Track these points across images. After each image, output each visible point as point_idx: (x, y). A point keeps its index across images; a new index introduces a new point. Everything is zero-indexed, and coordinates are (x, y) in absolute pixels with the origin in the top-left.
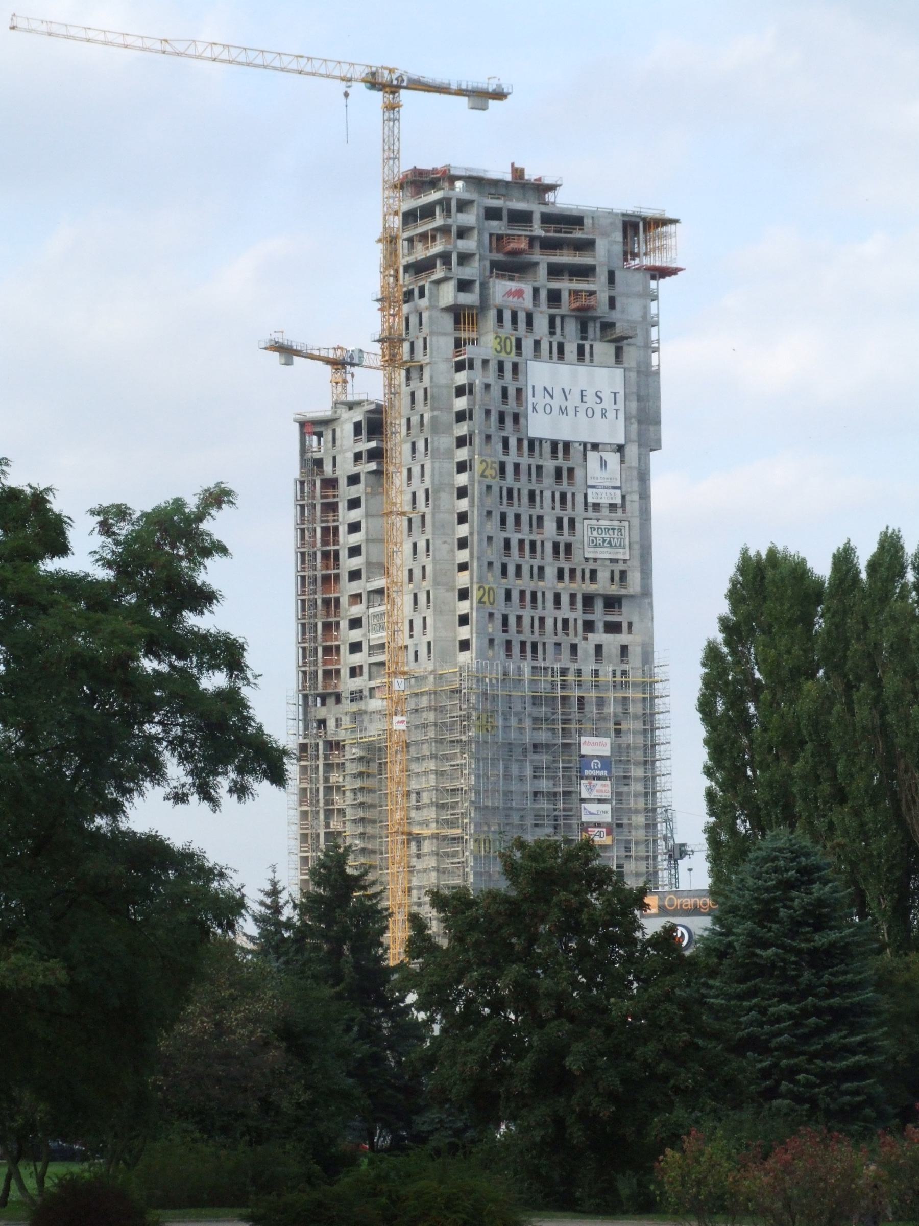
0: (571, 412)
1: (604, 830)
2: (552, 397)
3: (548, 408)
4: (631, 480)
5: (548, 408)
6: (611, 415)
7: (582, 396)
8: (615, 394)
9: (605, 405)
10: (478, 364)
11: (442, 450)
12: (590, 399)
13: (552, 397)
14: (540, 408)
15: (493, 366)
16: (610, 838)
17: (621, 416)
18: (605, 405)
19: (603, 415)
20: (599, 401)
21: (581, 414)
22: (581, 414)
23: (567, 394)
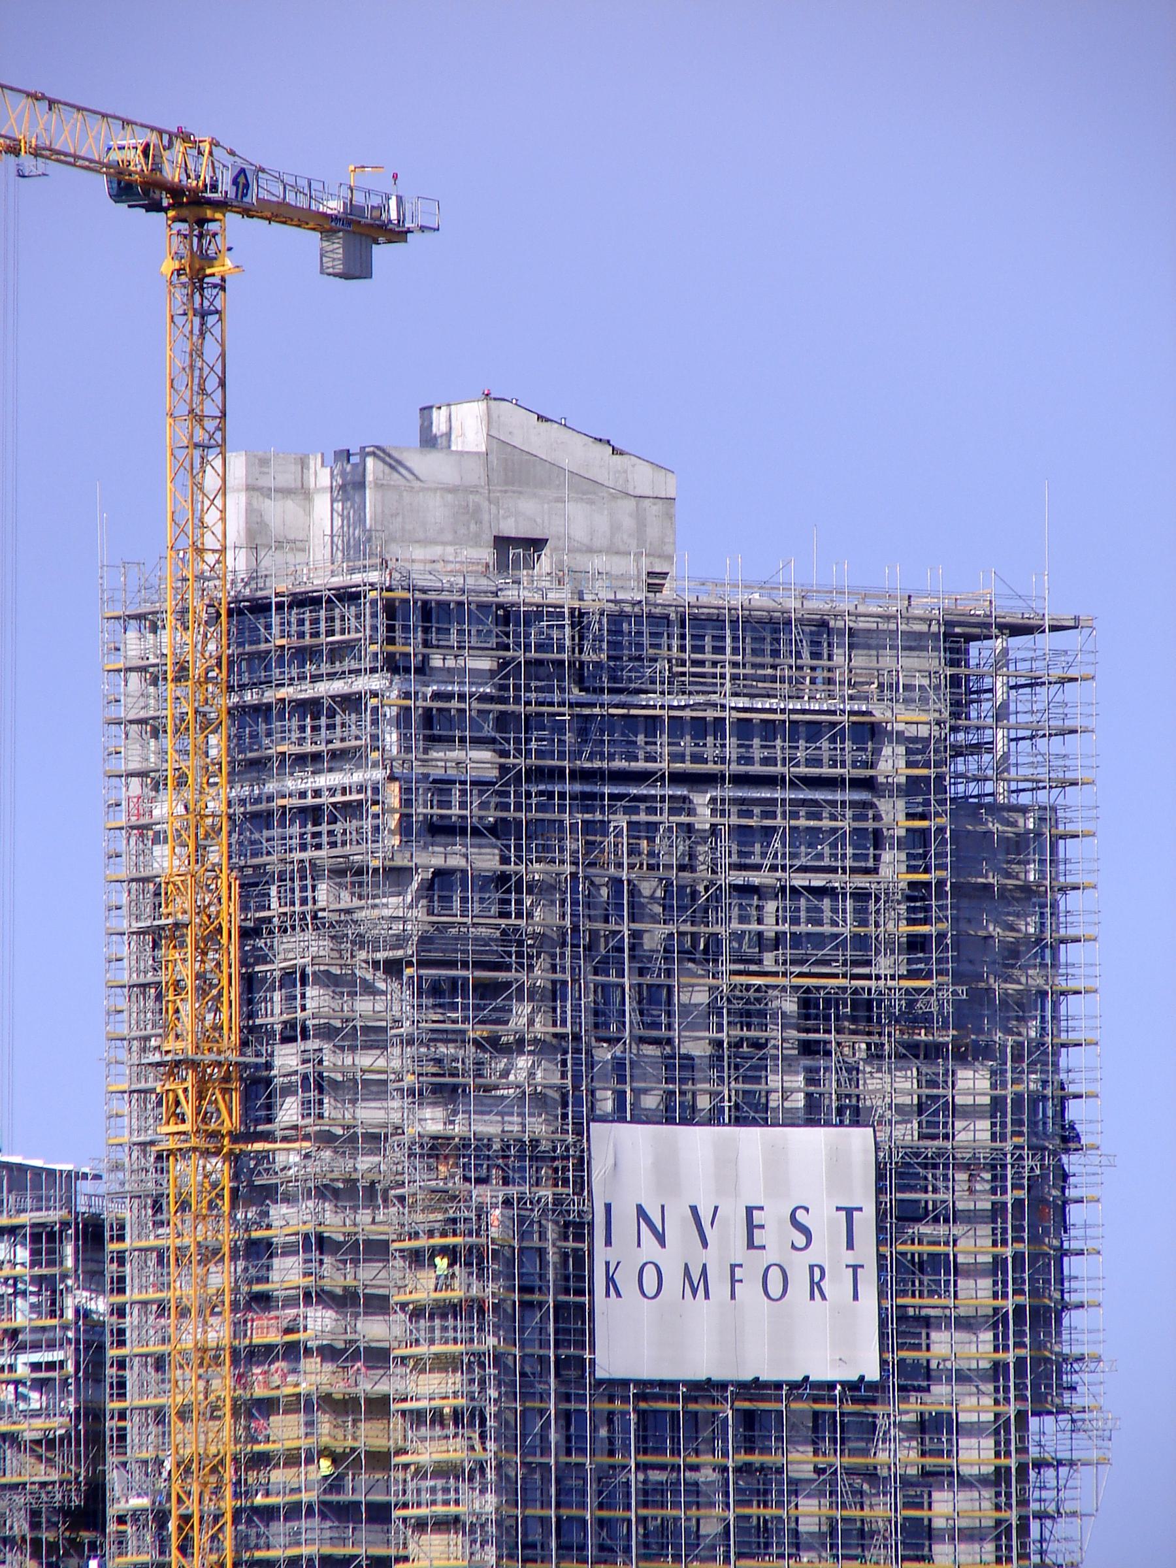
2: (661, 1239)
3: (650, 1275)
5: (650, 1275)
6: (837, 1286)
7: (751, 1227)
8: (849, 1212)
9: (818, 1253)
12: (775, 1235)
13: (661, 1239)
14: (626, 1279)
18: (818, 1253)
19: (816, 1288)
20: (801, 1240)
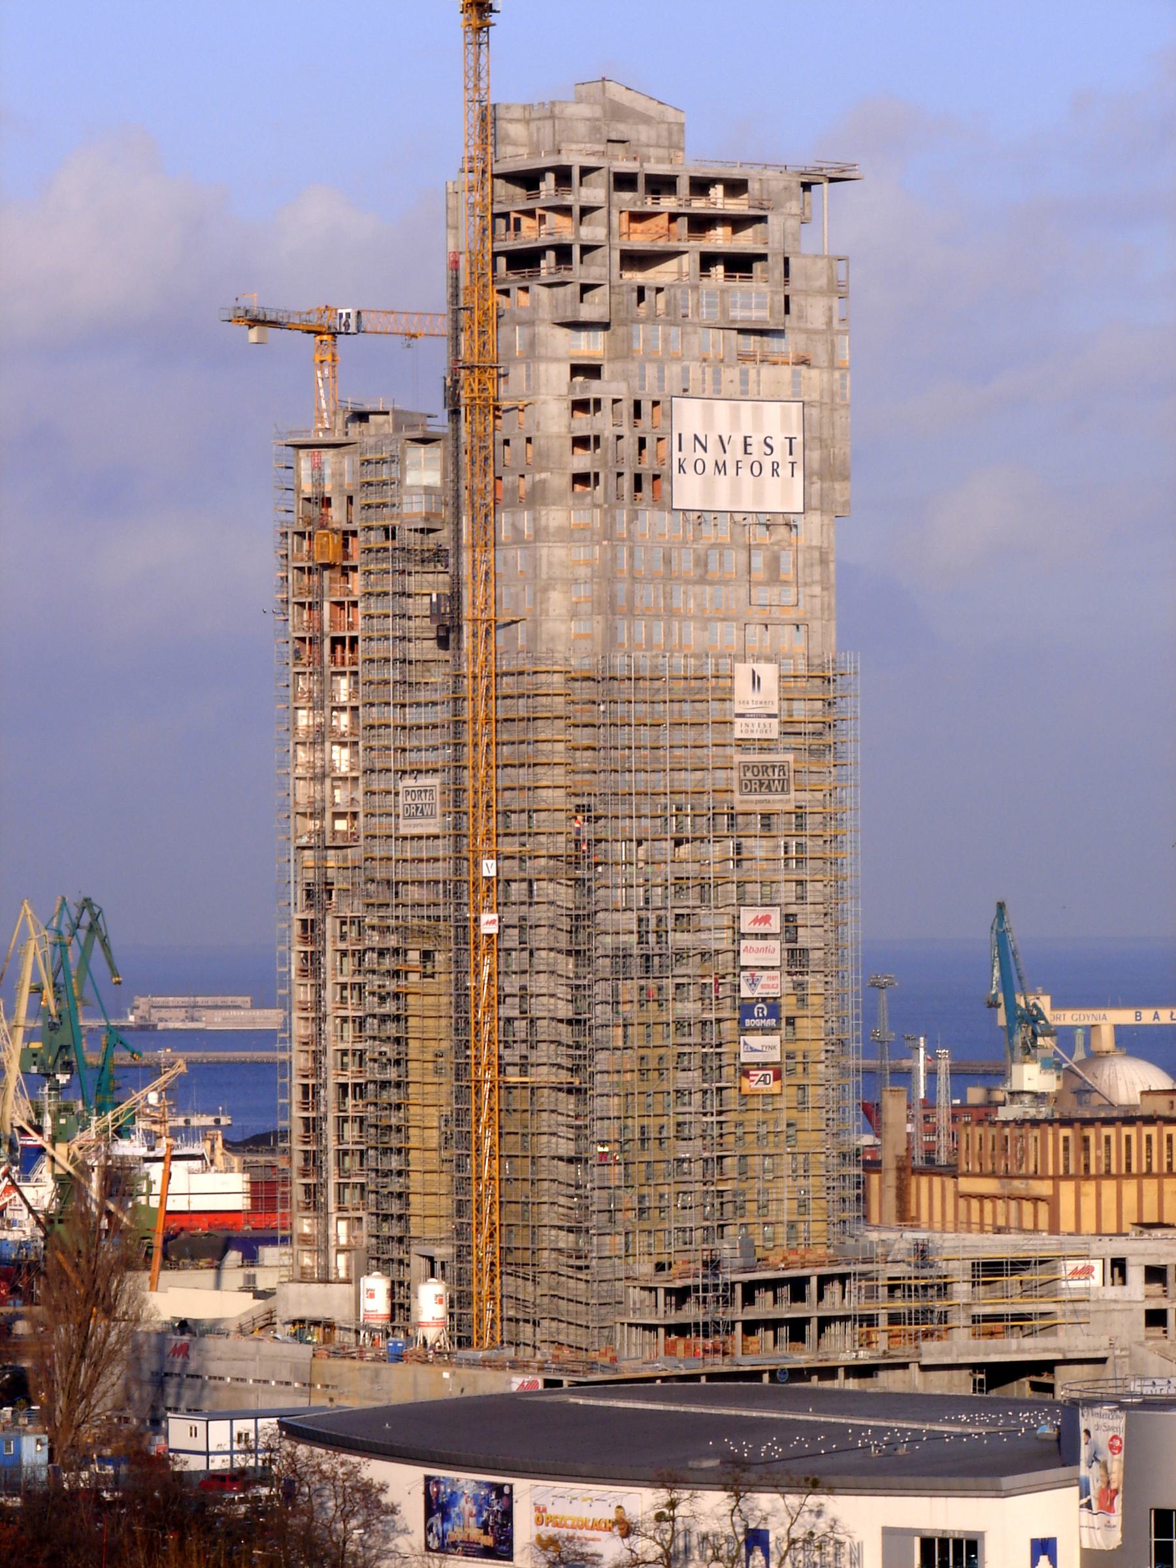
0: (731, 469)
1: (771, 1073)
3: (700, 464)
5: (700, 464)
7: (746, 445)
8: (791, 439)
10: (606, 405)
11: (552, 530)
12: (756, 448)
15: (626, 408)
16: (778, 1083)
20: (768, 451)
21: (745, 472)
22: (745, 472)
23: (726, 443)
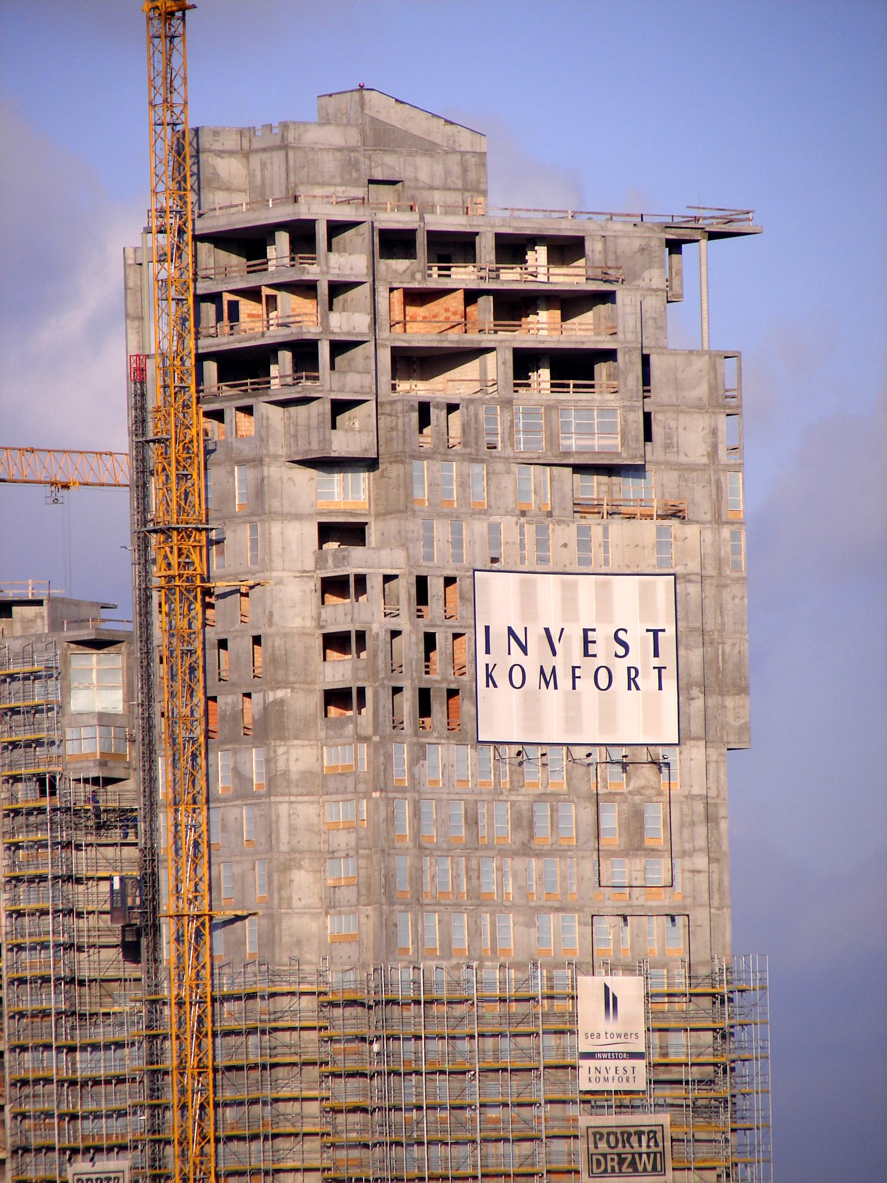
0: (564, 680)
2: (524, 649)
4: (693, 824)
12: (603, 647)
13: (524, 649)
14: (500, 676)
17: (670, 684)
19: (632, 682)
20: (621, 651)
22: (585, 683)
